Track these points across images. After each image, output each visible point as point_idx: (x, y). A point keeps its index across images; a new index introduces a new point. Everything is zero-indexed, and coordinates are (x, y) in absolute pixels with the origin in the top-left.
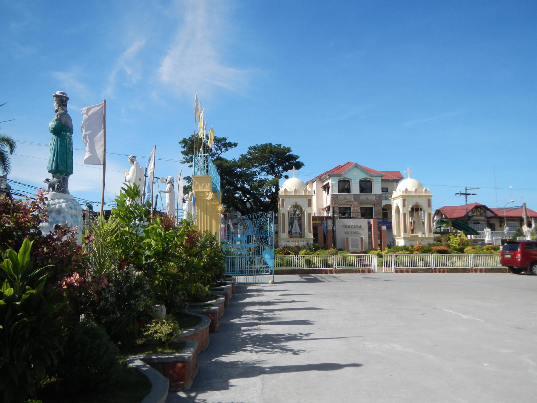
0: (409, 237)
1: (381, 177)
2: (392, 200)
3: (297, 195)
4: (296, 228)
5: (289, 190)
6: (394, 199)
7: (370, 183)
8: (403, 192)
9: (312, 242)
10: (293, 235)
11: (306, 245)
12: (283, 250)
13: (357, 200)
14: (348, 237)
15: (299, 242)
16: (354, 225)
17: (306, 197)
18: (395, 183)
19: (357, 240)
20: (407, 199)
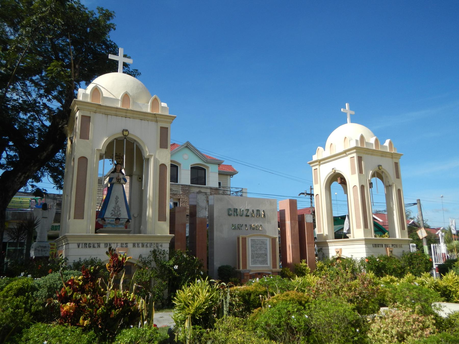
0: (373, 238)
1: (219, 164)
2: (318, 163)
3: (131, 108)
4: (117, 208)
5: (105, 94)
6: (321, 162)
7: (203, 171)
8: (357, 141)
9: (166, 247)
10: (109, 227)
11: (152, 258)
12: (82, 290)
13: (187, 193)
14: (244, 236)
15: (127, 247)
16: (251, 211)
17: (157, 121)
18: (229, 177)
19: (263, 243)
20: (364, 157)
